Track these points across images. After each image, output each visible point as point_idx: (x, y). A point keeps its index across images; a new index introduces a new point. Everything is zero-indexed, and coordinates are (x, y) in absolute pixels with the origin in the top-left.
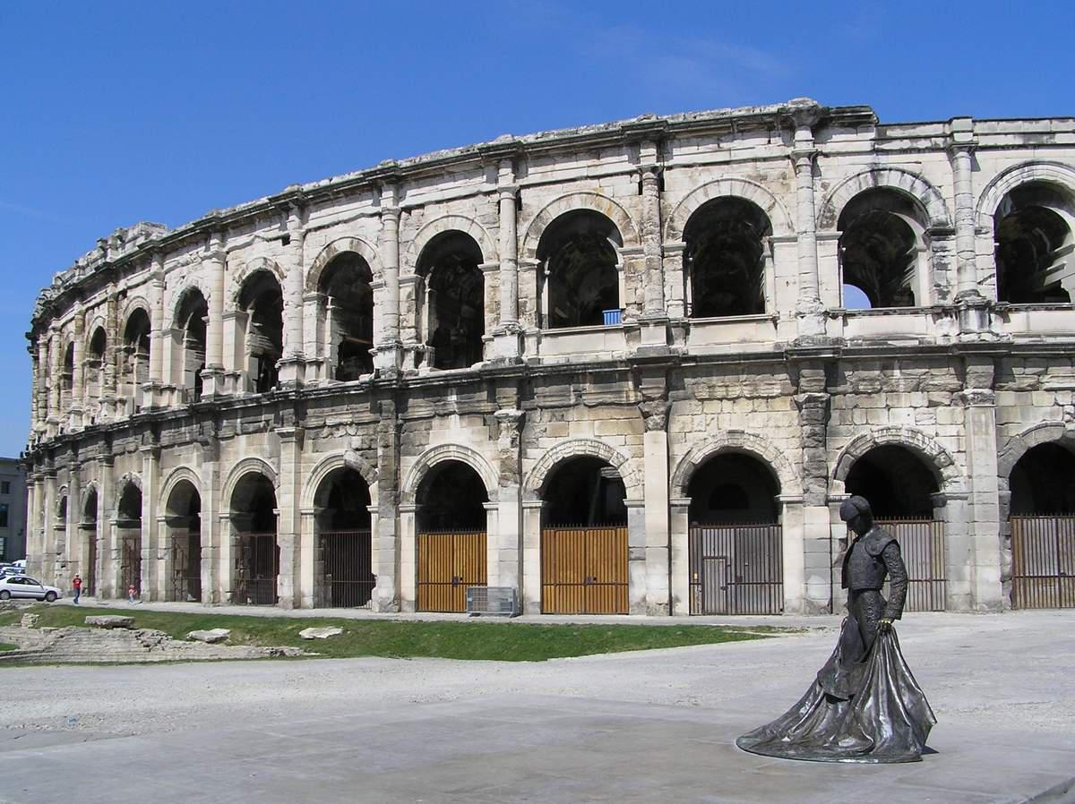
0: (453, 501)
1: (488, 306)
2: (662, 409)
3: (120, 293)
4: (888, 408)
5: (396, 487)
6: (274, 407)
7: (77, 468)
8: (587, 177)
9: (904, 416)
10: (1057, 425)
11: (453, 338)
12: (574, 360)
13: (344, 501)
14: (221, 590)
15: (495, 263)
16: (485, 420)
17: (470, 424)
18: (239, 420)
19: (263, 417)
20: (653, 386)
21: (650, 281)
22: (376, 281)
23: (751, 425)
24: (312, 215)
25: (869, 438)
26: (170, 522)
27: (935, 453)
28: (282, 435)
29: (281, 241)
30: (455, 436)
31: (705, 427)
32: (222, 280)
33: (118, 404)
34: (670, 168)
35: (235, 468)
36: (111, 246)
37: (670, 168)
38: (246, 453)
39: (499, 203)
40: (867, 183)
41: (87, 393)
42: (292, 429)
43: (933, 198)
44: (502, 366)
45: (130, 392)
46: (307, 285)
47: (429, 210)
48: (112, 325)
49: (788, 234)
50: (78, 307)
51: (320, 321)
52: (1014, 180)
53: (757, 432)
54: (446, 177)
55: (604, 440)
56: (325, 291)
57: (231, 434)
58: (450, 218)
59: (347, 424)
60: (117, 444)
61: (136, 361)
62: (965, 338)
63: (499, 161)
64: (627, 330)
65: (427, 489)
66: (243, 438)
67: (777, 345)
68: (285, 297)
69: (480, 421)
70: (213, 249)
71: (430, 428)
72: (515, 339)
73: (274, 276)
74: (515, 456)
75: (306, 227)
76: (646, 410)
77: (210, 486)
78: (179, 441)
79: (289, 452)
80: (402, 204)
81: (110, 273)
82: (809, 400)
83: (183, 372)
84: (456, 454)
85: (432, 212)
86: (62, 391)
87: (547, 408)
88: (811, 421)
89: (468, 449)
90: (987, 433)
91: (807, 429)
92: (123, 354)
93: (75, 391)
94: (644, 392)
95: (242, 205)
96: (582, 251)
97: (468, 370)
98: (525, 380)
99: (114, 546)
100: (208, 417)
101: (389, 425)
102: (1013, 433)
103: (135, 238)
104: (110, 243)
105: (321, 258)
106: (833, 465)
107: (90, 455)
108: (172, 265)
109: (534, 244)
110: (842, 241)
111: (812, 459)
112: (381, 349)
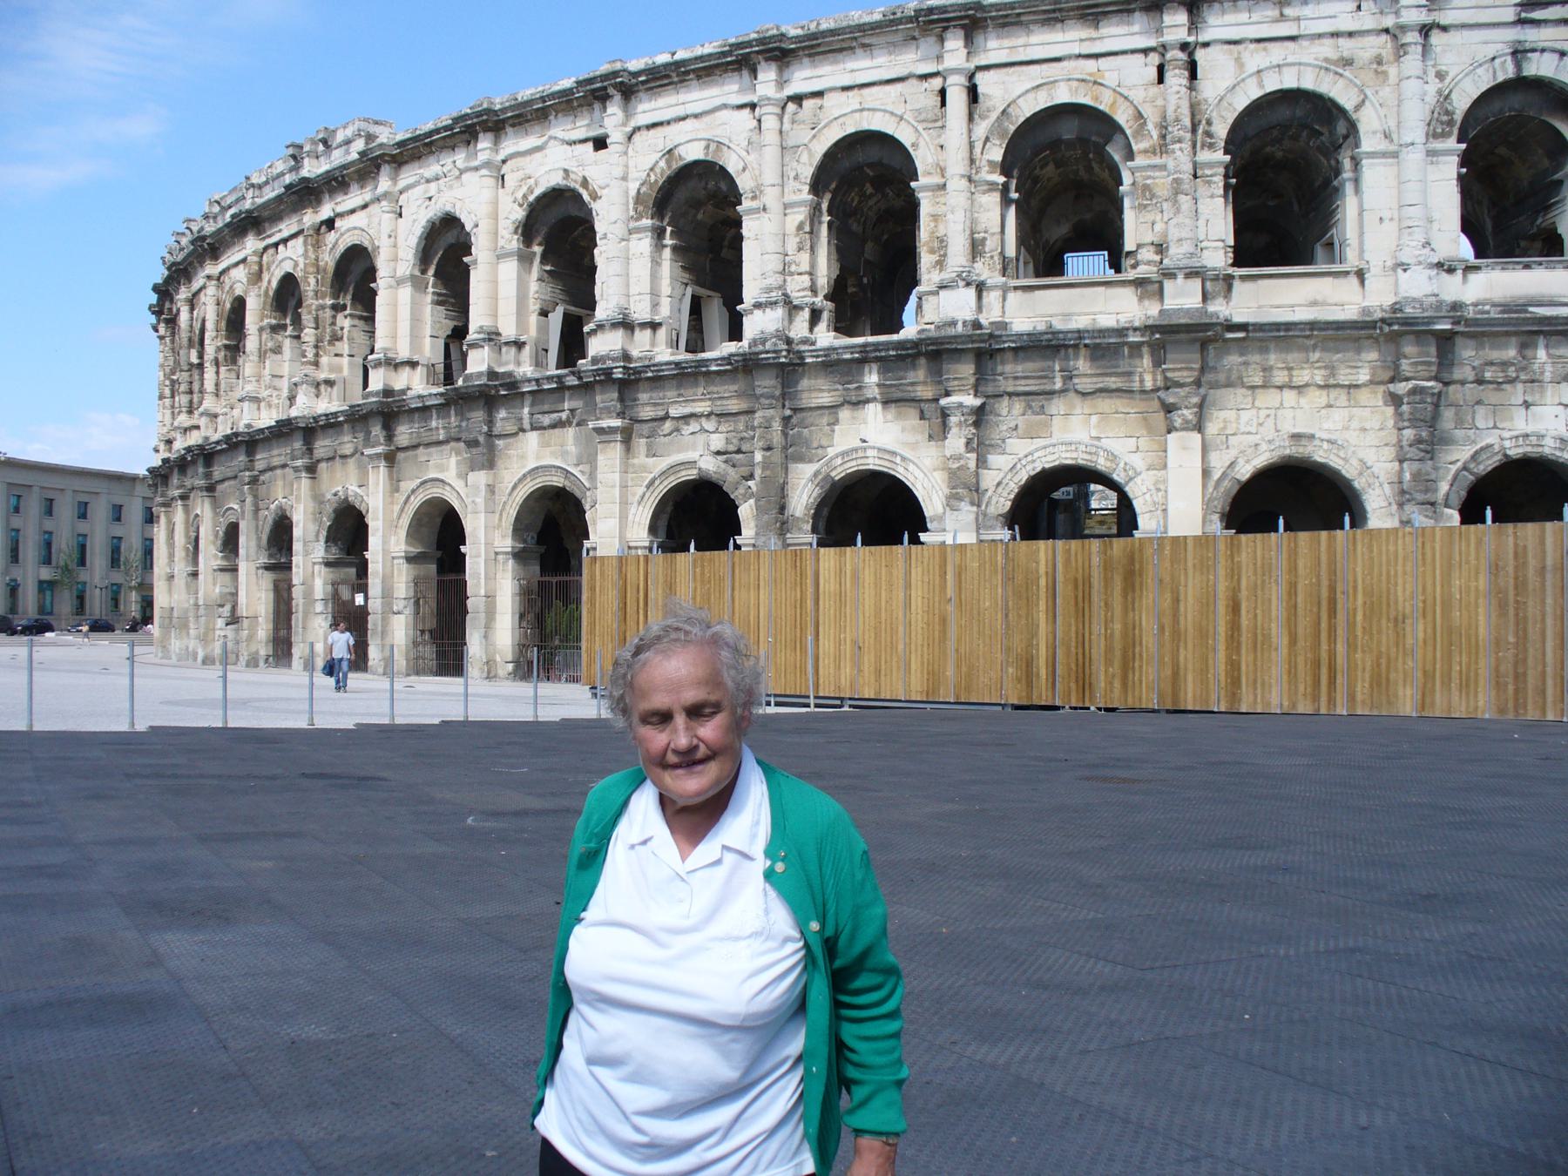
1: (927, 243)
2: (1195, 400)
3: (322, 223)
4: (1527, 405)
5: (782, 509)
6: (586, 388)
7: (254, 481)
8: (1080, 56)
11: (851, 290)
12: (1059, 325)
14: (498, 658)
15: (937, 180)
16: (922, 412)
17: (899, 416)
18: (526, 410)
19: (566, 406)
20: (1182, 366)
21: (1178, 211)
22: (746, 204)
23: (1325, 426)
24: (641, 107)
25: (1497, 448)
26: (410, 559)
28: (600, 431)
29: (590, 145)
30: (873, 435)
32: (495, 203)
33: (322, 387)
34: (1206, 45)
35: (520, 480)
36: (309, 154)
37: (1206, 45)
38: (538, 458)
39: (943, 93)
41: (267, 372)
42: (617, 423)
44: (951, 331)
45: (340, 369)
46: (636, 210)
47: (829, 100)
48: (311, 269)
49: (1383, 146)
50: (251, 244)
51: (656, 263)
53: (1333, 437)
54: (859, 51)
55: (1105, 443)
56: (662, 219)
57: (514, 429)
58: (865, 113)
59: (702, 415)
60: (322, 446)
61: (347, 323)
63: (945, 29)
64: (1139, 283)
65: (825, 512)
66: (532, 438)
67: (1366, 311)
68: (600, 227)
69: (913, 413)
70: (483, 157)
71: (836, 422)
72: (971, 293)
73: (580, 196)
74: (972, 465)
75: (633, 124)
76: (1171, 400)
77: (481, 507)
78: (427, 440)
79: (610, 457)
80: (790, 90)
81: (305, 193)
82: (1414, 391)
83: (428, 340)
84: (878, 462)
86: (223, 369)
87: (1018, 394)
88: (1414, 422)
89: (894, 453)
91: (1409, 434)
92: (329, 313)
93: (248, 365)
94: (1169, 375)
95: (529, 92)
96: (1057, 166)
97: (895, 337)
98: (985, 350)
100: (476, 404)
101: (772, 418)
103: (348, 142)
104: (307, 148)
105: (658, 170)
106: (1444, 487)
107: (276, 461)
108: (411, 180)
109: (997, 154)
110: (1465, 160)
111: (1416, 477)
112: (758, 306)
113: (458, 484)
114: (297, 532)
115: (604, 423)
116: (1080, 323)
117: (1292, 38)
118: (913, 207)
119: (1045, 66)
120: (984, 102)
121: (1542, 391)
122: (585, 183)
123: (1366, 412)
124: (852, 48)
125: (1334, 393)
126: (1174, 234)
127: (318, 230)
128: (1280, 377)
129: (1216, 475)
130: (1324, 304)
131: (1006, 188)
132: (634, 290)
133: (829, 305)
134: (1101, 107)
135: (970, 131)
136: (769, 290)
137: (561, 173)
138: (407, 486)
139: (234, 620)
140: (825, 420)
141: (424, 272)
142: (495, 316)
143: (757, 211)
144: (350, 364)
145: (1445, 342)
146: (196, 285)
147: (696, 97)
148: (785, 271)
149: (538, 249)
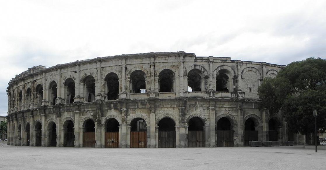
0: (113, 126)
3: (34, 80)
4: (196, 110)
5: (100, 123)
9: (199, 112)
10: (226, 114)
13: (89, 126)
17: (116, 111)
27: (204, 119)
28: (75, 112)
29: (74, 72)
30: (113, 114)
31: (162, 113)
34: (156, 63)
37: (156, 63)
38: (67, 116)
39: (122, 68)
40: (193, 68)
43: (205, 71)
51: (84, 89)
52: (220, 69)
62: (210, 98)
66: (66, 113)
67: (176, 98)
69: (118, 111)
70: (59, 73)
72: (125, 95)
74: (125, 117)
79: (77, 117)
80: (102, 66)
83: (51, 99)
85: (108, 68)
86: (19, 101)
88: (182, 112)
90: (213, 115)
97: (116, 100)
100: (58, 109)
102: (218, 115)
106: (186, 121)
109: (129, 76)
110: (188, 79)
112: (97, 96)
113: (55, 119)
114: (31, 126)
115: (76, 111)
116: (140, 99)
117: (167, 62)
118: (118, 83)
119: (135, 65)
120: (128, 69)
121: (198, 108)
122: (73, 78)
123: (176, 111)
125: (172, 108)
127: (34, 82)
128: (165, 106)
129: (157, 119)
130: (171, 97)
131: (130, 81)
132: (81, 93)
133: (107, 96)
135: (126, 73)
136: (99, 94)
138: (48, 119)
139: (20, 139)
140: (106, 111)
141: (50, 89)
142: (61, 95)
143: (97, 83)
144: (39, 102)
145: (186, 102)
146: (14, 88)
147: (89, 66)
148: (101, 91)
149: (67, 86)
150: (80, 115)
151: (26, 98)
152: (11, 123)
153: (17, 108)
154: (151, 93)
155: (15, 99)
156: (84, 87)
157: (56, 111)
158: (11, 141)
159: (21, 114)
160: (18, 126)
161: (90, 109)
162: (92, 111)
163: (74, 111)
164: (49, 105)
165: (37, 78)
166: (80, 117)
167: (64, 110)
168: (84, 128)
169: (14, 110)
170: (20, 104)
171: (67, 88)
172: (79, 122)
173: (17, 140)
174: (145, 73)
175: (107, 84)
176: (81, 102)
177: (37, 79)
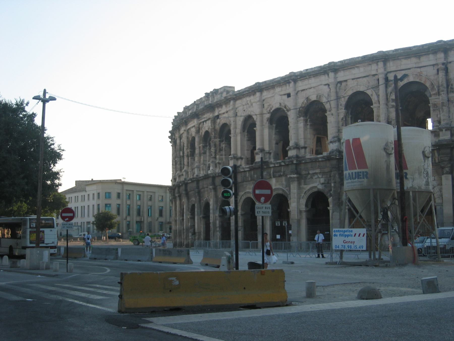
2: (449, 165)
21: (443, 111)
22: (328, 113)
28: (291, 178)
29: (286, 96)
38: (276, 185)
39: (378, 80)
41: (202, 159)
51: (305, 129)
54: (356, 69)
59: (318, 173)
63: (378, 62)
68: (290, 119)
70: (258, 99)
76: (443, 166)
80: (339, 79)
83: (246, 151)
86: (190, 158)
99: (218, 225)
109: (393, 97)
112: (331, 142)
114: (211, 207)
115: (292, 176)
122: (285, 107)
124: (354, 68)
126: (442, 118)
134: (422, 82)
135: (386, 91)
136: (334, 137)
137: (279, 104)
139: (194, 233)
141: (244, 131)
147: (313, 82)
149: (274, 125)
150: (299, 184)
151: (202, 151)
152: (178, 203)
153: (187, 173)
154: (442, 130)
155: (183, 153)
156: (306, 125)
157: (255, 176)
158: (178, 238)
159: (194, 185)
160: (190, 207)
161: (318, 171)
162: (323, 173)
163: (288, 176)
164: (243, 165)
165: (219, 111)
166: (299, 188)
167: (270, 175)
168: (308, 209)
169: (183, 175)
170: (192, 164)
171: (274, 128)
172: (299, 198)
173: (189, 236)
174: (426, 88)
175: (350, 116)
176: (300, 156)
177: (220, 113)
